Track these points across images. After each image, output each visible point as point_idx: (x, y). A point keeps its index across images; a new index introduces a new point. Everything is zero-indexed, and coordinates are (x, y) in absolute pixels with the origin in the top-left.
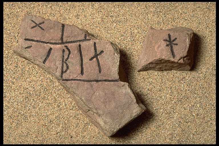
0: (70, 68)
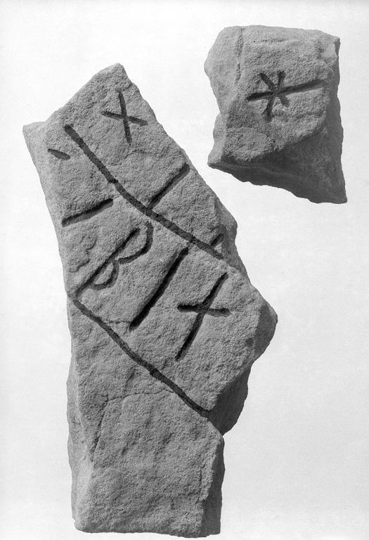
0: (115, 286)
